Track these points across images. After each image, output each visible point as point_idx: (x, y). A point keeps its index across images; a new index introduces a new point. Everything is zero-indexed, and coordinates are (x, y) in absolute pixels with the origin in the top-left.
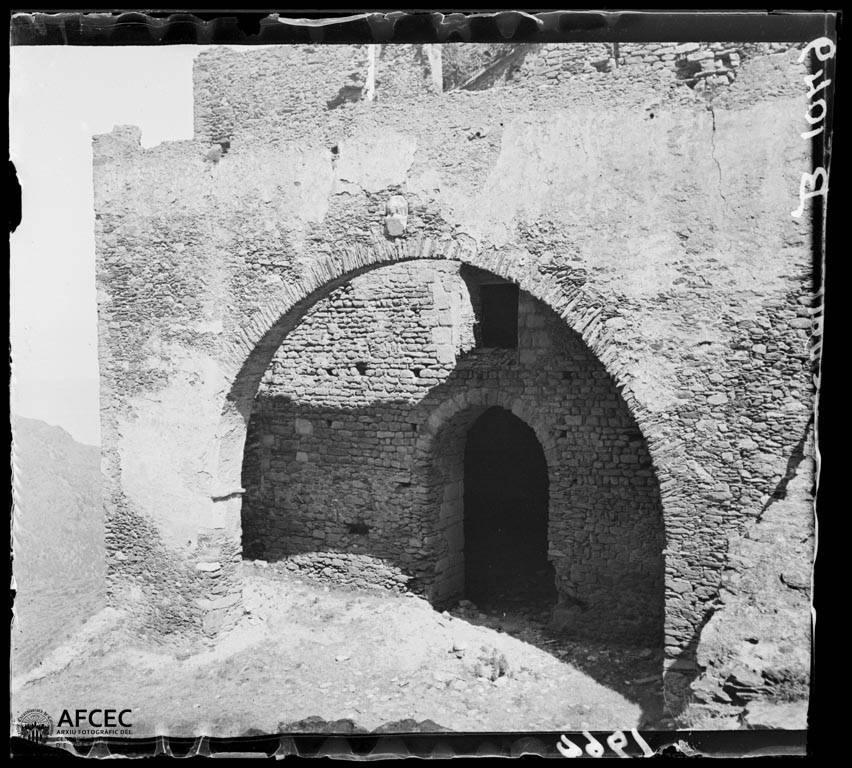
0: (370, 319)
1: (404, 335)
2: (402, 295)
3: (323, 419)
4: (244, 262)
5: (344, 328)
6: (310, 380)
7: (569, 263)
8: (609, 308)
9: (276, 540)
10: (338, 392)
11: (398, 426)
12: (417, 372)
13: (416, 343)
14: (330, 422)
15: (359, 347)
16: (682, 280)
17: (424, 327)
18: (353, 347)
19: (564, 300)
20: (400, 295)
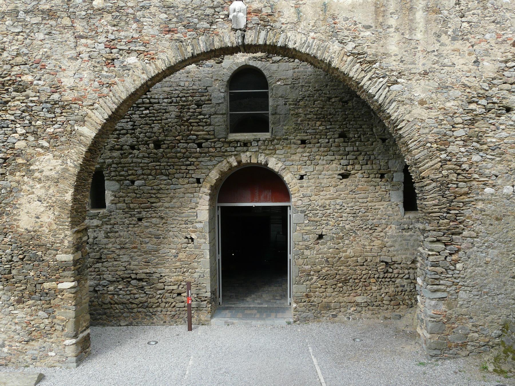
0: (164, 111)
3: (128, 180)
4: (103, 48)
5: (144, 117)
6: (116, 154)
7: (365, 49)
8: (393, 78)
11: (186, 181)
12: (200, 145)
13: (199, 126)
14: (133, 182)
15: (155, 129)
16: (437, 62)
17: (205, 115)
18: (151, 130)
19: (363, 74)
20: (187, 95)
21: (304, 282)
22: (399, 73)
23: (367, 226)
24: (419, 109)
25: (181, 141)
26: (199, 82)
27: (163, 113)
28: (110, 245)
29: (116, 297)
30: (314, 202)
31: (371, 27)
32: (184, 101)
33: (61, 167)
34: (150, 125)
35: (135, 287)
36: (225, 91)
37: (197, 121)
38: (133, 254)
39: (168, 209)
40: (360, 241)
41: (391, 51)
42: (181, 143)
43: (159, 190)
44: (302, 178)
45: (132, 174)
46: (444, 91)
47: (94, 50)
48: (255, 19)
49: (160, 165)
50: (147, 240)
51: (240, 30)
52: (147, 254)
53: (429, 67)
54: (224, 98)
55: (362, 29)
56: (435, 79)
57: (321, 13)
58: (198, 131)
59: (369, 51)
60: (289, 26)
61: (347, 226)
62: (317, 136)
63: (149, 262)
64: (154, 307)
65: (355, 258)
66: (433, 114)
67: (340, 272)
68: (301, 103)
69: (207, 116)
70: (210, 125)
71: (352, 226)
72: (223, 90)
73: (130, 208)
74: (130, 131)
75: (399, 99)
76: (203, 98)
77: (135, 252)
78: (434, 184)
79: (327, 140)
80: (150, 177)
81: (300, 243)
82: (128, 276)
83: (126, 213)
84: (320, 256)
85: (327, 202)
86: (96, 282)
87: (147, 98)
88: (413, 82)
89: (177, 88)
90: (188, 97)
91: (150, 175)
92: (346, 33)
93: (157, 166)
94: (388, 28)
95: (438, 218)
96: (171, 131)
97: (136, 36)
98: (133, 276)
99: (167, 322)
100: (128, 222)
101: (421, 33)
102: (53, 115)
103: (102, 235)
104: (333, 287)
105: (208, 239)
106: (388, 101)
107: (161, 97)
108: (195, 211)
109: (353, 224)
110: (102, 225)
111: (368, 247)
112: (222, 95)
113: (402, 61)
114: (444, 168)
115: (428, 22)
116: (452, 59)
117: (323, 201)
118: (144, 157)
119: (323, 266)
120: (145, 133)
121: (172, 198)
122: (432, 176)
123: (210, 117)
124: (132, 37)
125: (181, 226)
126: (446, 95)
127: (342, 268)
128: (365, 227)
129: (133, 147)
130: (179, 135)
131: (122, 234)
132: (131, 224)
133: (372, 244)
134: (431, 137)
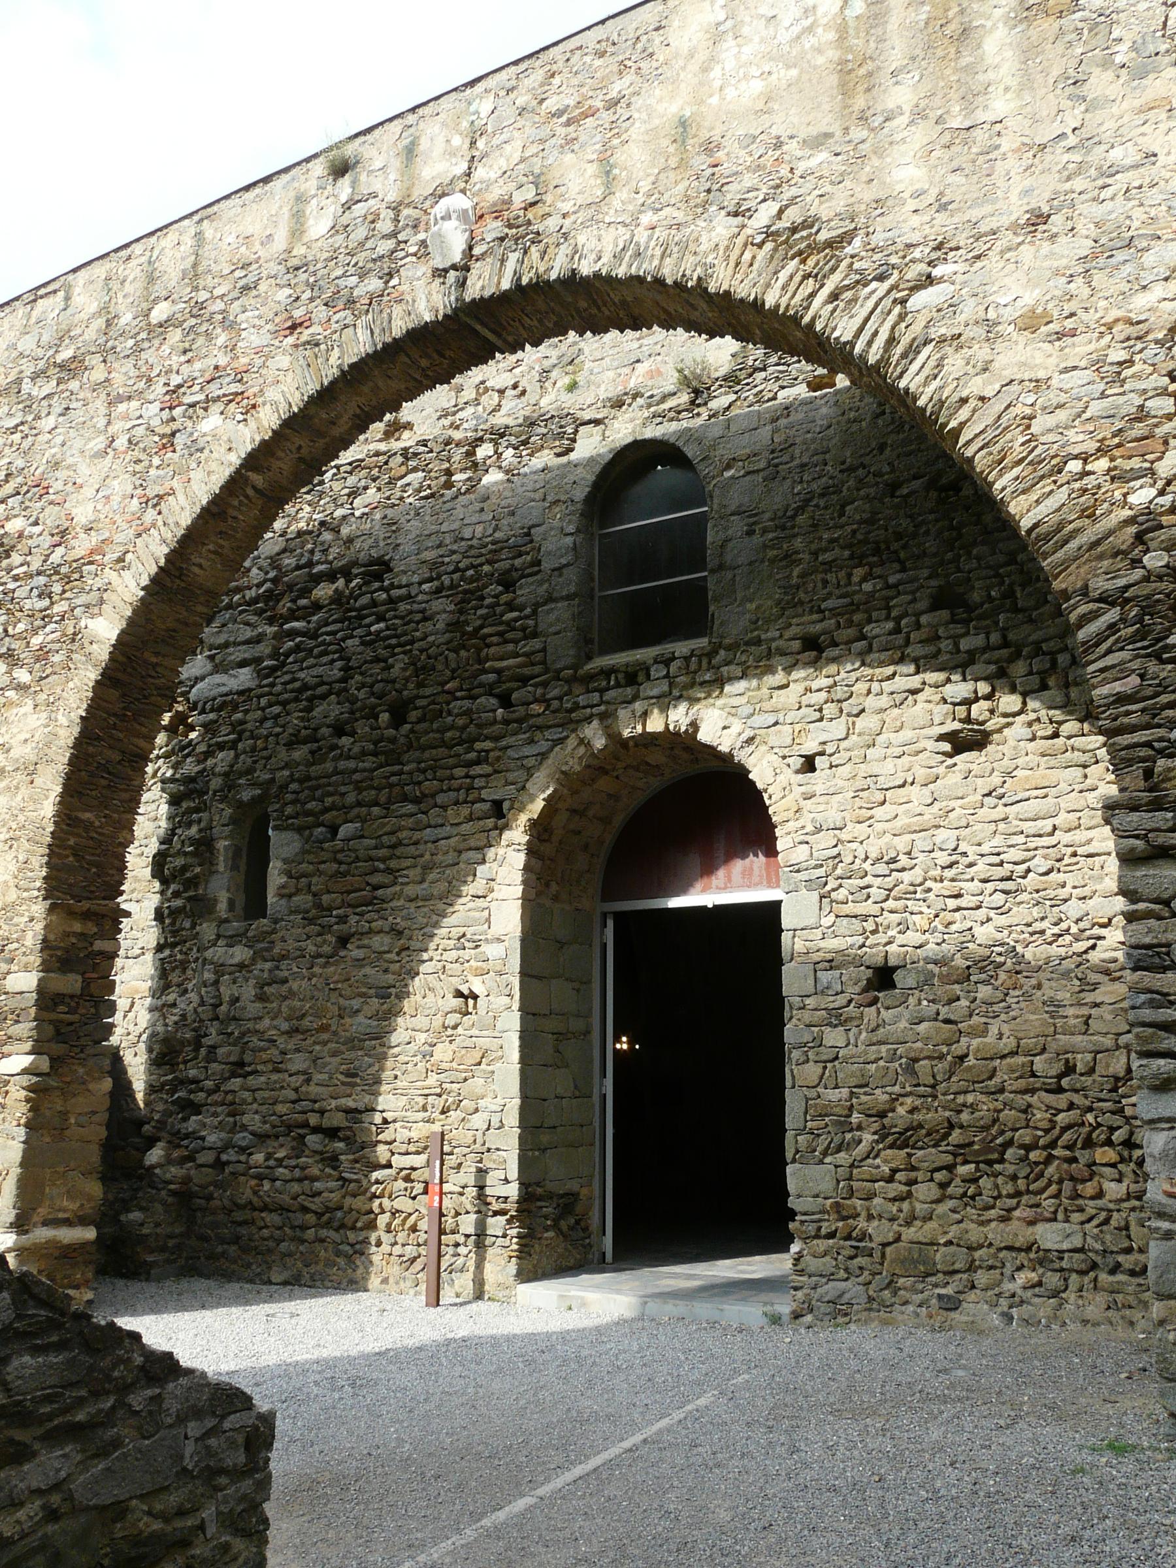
0: (418, 617)
1: (485, 631)
2: (483, 559)
3: (322, 824)
6: (300, 753)
9: (217, 1089)
10: (352, 764)
11: (465, 811)
12: (505, 701)
13: (506, 642)
14: (334, 830)
16: (1081, 168)
17: (521, 609)
20: (479, 561)
21: (825, 1153)
22: (938, 248)
23: (1064, 926)
24: (1021, 346)
25: (458, 694)
26: (511, 520)
27: (418, 623)
28: (267, 1022)
29: (267, 1185)
30: (854, 846)
31: (828, 135)
32: (471, 580)
33: (46, 730)
34: (385, 661)
35: (318, 1157)
36: (578, 531)
37: (501, 628)
38: (318, 1048)
39: (413, 905)
40: (1039, 986)
41: (899, 188)
42: (457, 699)
43: (393, 847)
44: (809, 765)
45: (333, 808)
46: (1120, 256)
47: (140, 421)
48: (493, 228)
49: (401, 773)
50: (356, 1003)
51: (454, 267)
52: (353, 1048)
53: (1047, 195)
54: (575, 548)
55: (799, 154)
56: (1079, 227)
57: (672, 149)
58: (502, 659)
59: (825, 212)
60: (581, 216)
61: (978, 931)
62: (857, 617)
63: (355, 1075)
64: (359, 1225)
65: (1020, 1059)
66: (1081, 349)
67: (965, 1117)
68: (801, 519)
69: (528, 611)
70: (535, 635)
71: (999, 930)
72: (571, 529)
73: (319, 906)
74: (337, 686)
75: (943, 331)
76: (518, 562)
77: (325, 1043)
78: (1113, 615)
79: (890, 625)
80: (376, 810)
81: (807, 1001)
82: (300, 1118)
83: (311, 921)
84: (884, 1048)
85: (902, 843)
86: (223, 1135)
87: (381, 589)
88: (993, 262)
89: (455, 547)
90: (481, 565)
91: (377, 804)
92: (749, 180)
93: (393, 774)
94: (887, 120)
95: (1144, 752)
96: (433, 668)
97: (222, 361)
98: (313, 1120)
99: (391, 1280)
100: (312, 948)
101: (1008, 96)
102: (46, 602)
103: (248, 991)
104: (939, 1176)
105: (517, 996)
106: (899, 350)
107: (416, 579)
108: (486, 905)
109: (1002, 921)
110: (253, 960)
111: (1070, 1011)
112: (569, 540)
113: (943, 207)
114: (1152, 545)
115: (1028, 53)
116: (1140, 140)
117: (888, 838)
118: (364, 753)
119: (897, 1089)
120: (372, 686)
121: (427, 868)
122: (1100, 584)
123: (535, 612)
124: (216, 367)
125: (446, 956)
126: (1128, 269)
127: (970, 1098)
128: (1056, 930)
129: (339, 730)
130: (453, 678)
131: (295, 985)
132: (319, 956)
133: (1089, 998)
134: (1081, 437)
